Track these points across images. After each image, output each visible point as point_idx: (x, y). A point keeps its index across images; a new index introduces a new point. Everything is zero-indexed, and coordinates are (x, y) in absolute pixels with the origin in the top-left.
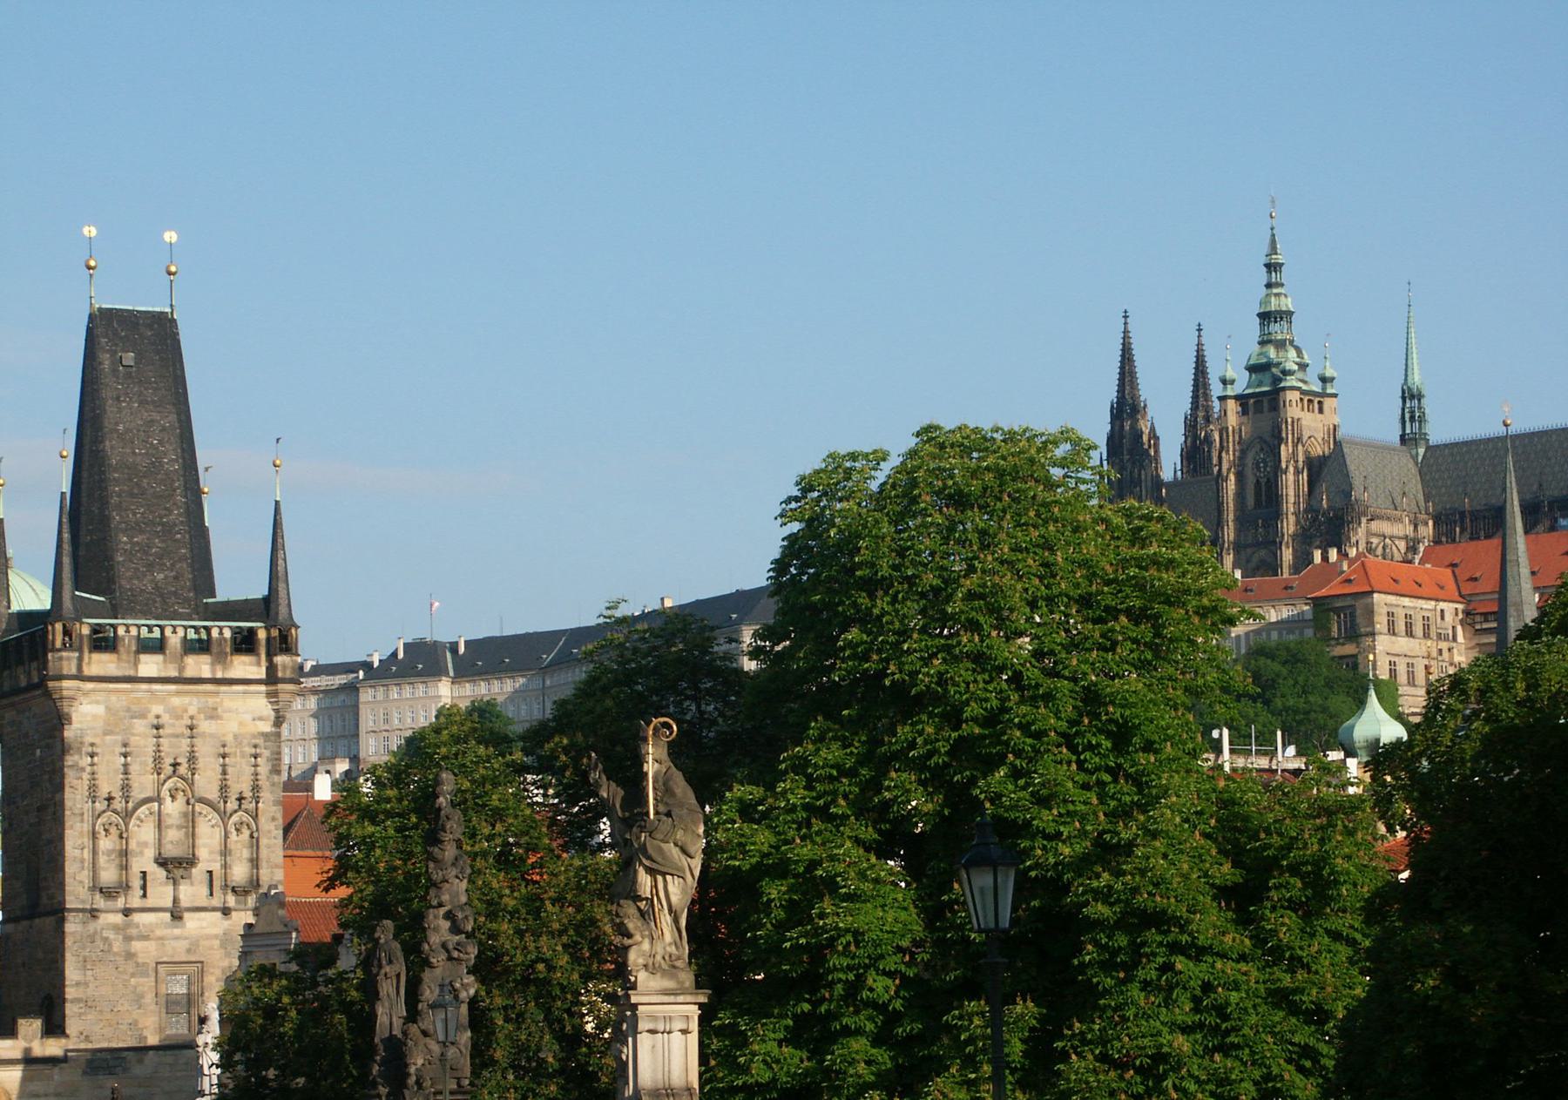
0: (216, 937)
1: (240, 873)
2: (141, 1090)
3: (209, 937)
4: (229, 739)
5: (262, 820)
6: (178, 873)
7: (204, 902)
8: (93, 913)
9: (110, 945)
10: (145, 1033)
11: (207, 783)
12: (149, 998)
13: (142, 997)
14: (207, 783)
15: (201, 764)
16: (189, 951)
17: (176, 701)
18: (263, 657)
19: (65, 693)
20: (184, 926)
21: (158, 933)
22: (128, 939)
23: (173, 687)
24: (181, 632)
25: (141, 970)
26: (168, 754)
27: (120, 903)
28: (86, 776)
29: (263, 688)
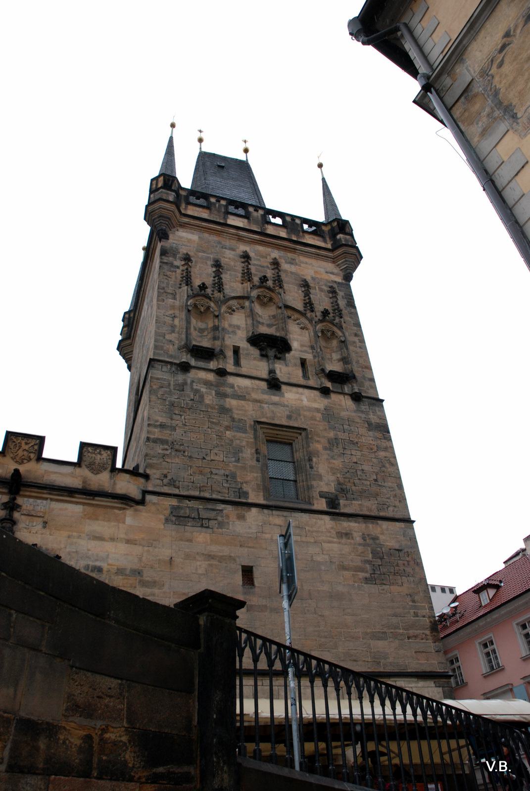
0: (318, 410)
1: (334, 366)
2: (246, 549)
3: (310, 409)
4: (309, 279)
5: (347, 334)
6: (271, 353)
7: (302, 382)
8: (185, 367)
9: (202, 397)
10: (246, 488)
11: (294, 297)
12: (248, 453)
13: (242, 452)
14: (294, 297)
15: (286, 286)
16: (289, 417)
17: (261, 248)
18: (328, 239)
19: (164, 212)
20: (283, 395)
21: (254, 396)
22: (222, 395)
23: (258, 237)
24: (261, 212)
25: (237, 425)
26: (255, 275)
27: (213, 365)
28: (179, 271)
29: (330, 254)
